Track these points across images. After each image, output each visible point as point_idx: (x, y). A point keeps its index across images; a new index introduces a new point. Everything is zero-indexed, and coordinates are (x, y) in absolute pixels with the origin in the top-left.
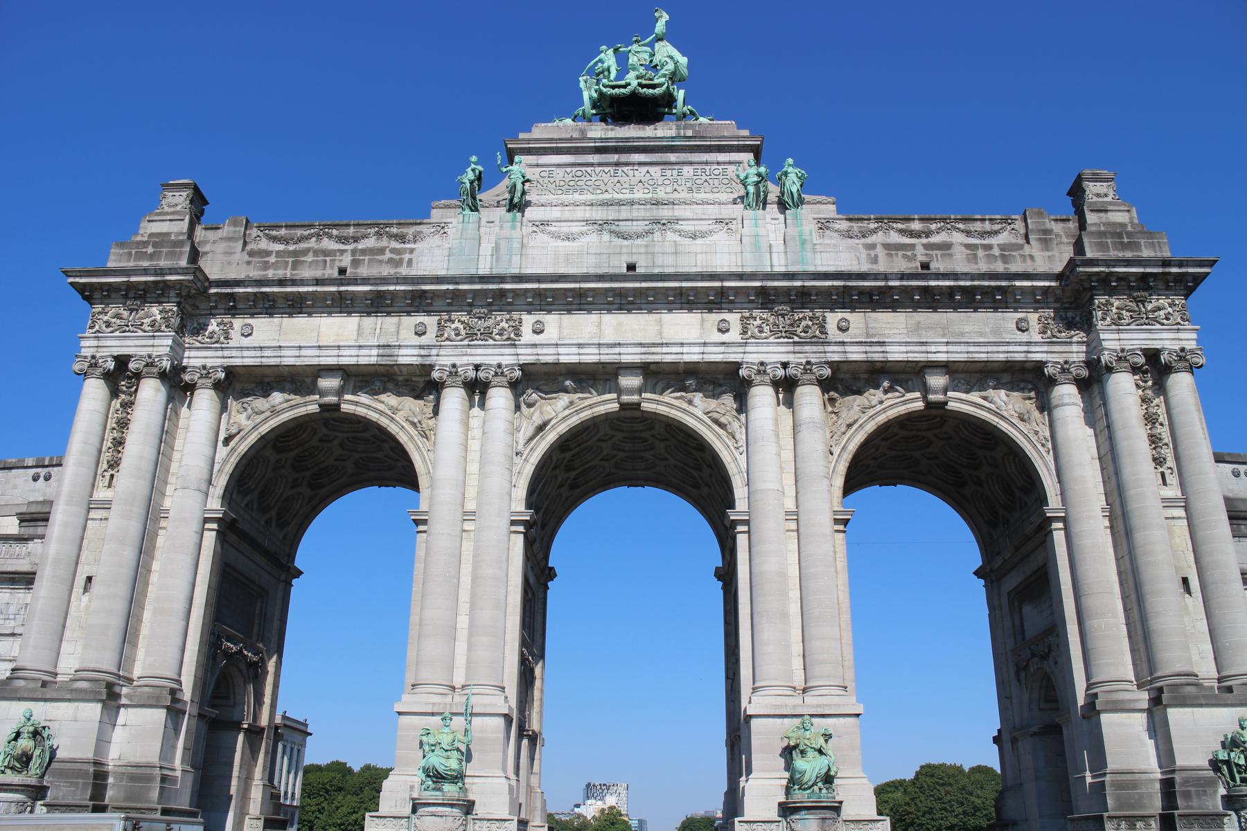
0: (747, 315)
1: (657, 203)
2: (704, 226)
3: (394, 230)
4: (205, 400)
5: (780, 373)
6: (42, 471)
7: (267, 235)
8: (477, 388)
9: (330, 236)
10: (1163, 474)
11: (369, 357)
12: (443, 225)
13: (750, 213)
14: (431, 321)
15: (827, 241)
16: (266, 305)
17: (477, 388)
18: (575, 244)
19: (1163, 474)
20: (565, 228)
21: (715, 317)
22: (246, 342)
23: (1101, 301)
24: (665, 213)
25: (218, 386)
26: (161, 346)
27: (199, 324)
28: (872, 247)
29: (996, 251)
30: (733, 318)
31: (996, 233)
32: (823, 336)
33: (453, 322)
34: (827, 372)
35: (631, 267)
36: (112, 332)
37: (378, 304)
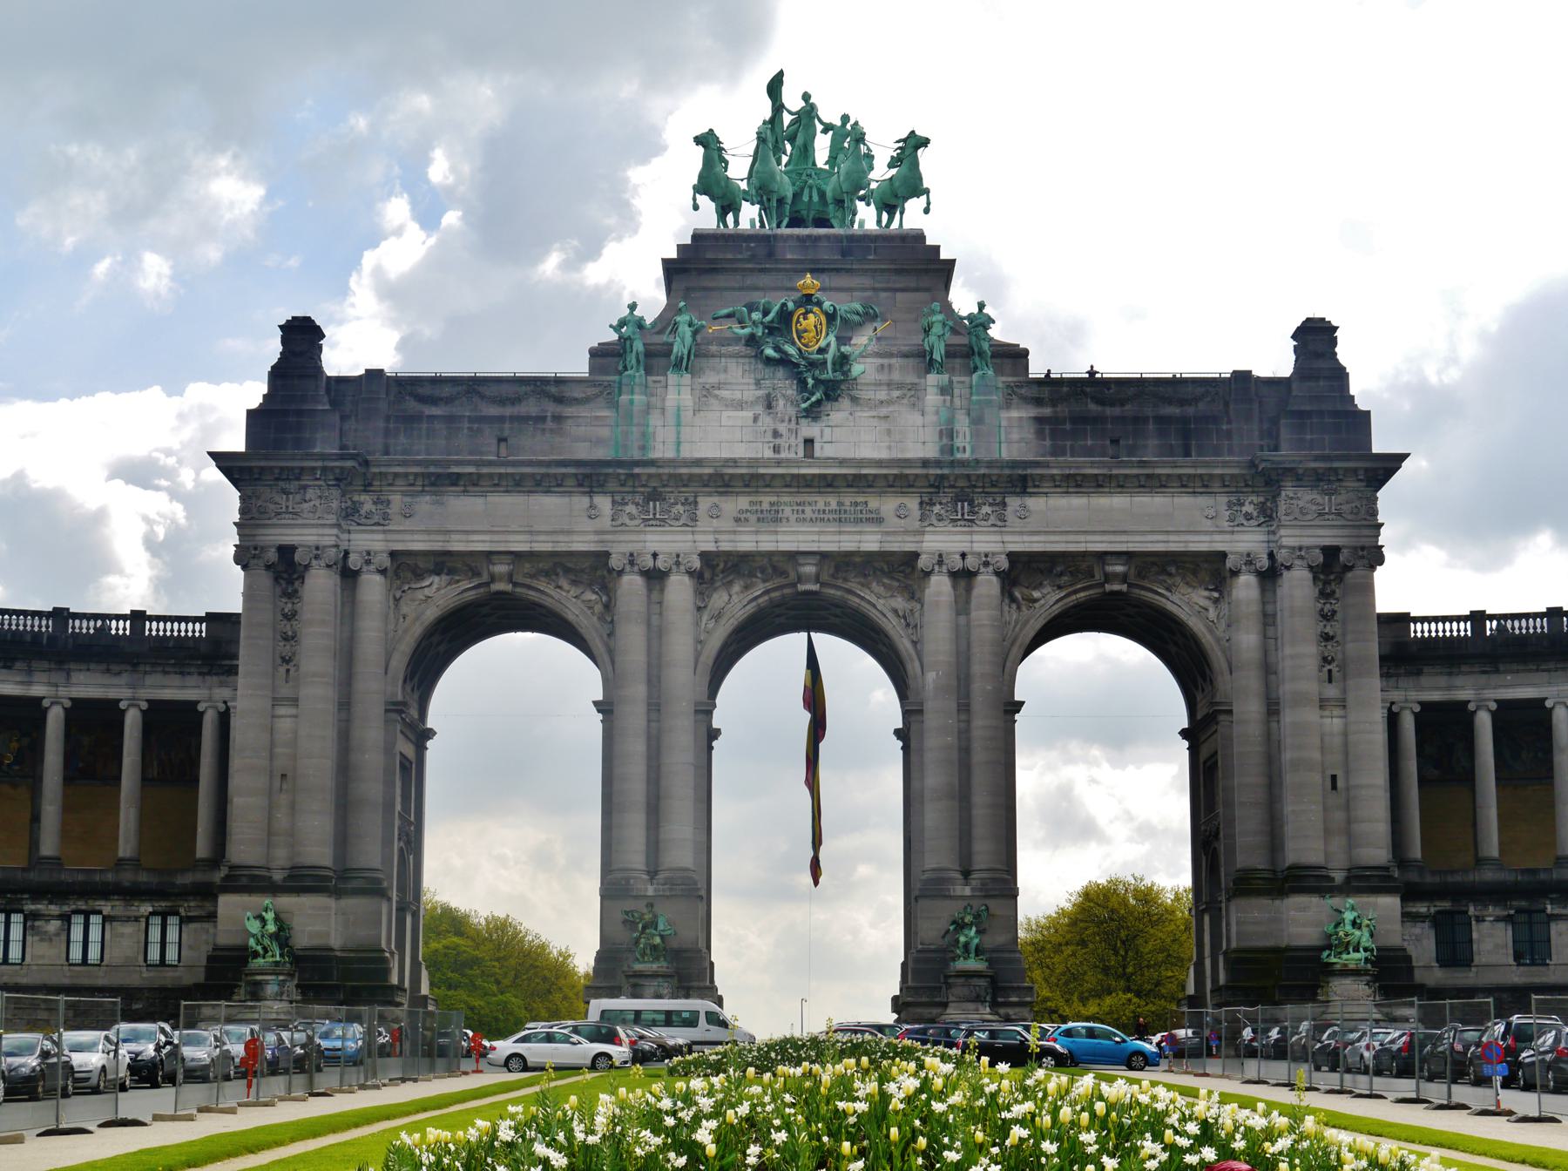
0: (926, 499)
3: (553, 389)
4: (373, 587)
5: (958, 565)
7: (411, 394)
9: (482, 397)
10: (1330, 671)
12: (606, 383)
17: (655, 577)
19: (1330, 671)
22: (407, 525)
23: (1288, 493)
25: (383, 572)
26: (327, 537)
27: (354, 502)
31: (1196, 400)
32: (1003, 524)
33: (627, 504)
36: (269, 519)
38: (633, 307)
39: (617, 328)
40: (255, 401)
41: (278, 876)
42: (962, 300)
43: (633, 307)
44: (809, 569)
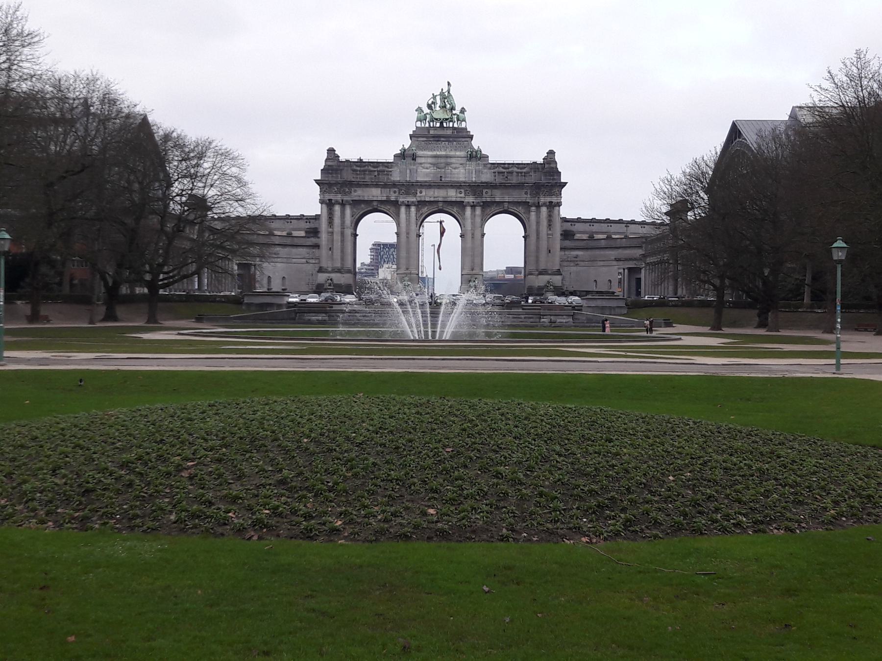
1: (447, 157)
2: (457, 166)
6: (308, 221)
8: (408, 206)
9: (371, 166)
11: (384, 198)
13: (468, 163)
14: (397, 190)
15: (485, 171)
16: (359, 185)
17: (408, 206)
18: (428, 170)
20: (426, 165)
21: (458, 190)
22: (356, 194)
24: (449, 160)
26: (339, 197)
28: (494, 173)
29: (523, 174)
30: (462, 190)
31: (525, 168)
34: (482, 204)
35: (441, 177)
37: (385, 186)
38: (403, 145)
39: (400, 150)
40: (322, 168)
41: (330, 269)
42: (475, 144)
43: (403, 145)
44: (440, 204)
